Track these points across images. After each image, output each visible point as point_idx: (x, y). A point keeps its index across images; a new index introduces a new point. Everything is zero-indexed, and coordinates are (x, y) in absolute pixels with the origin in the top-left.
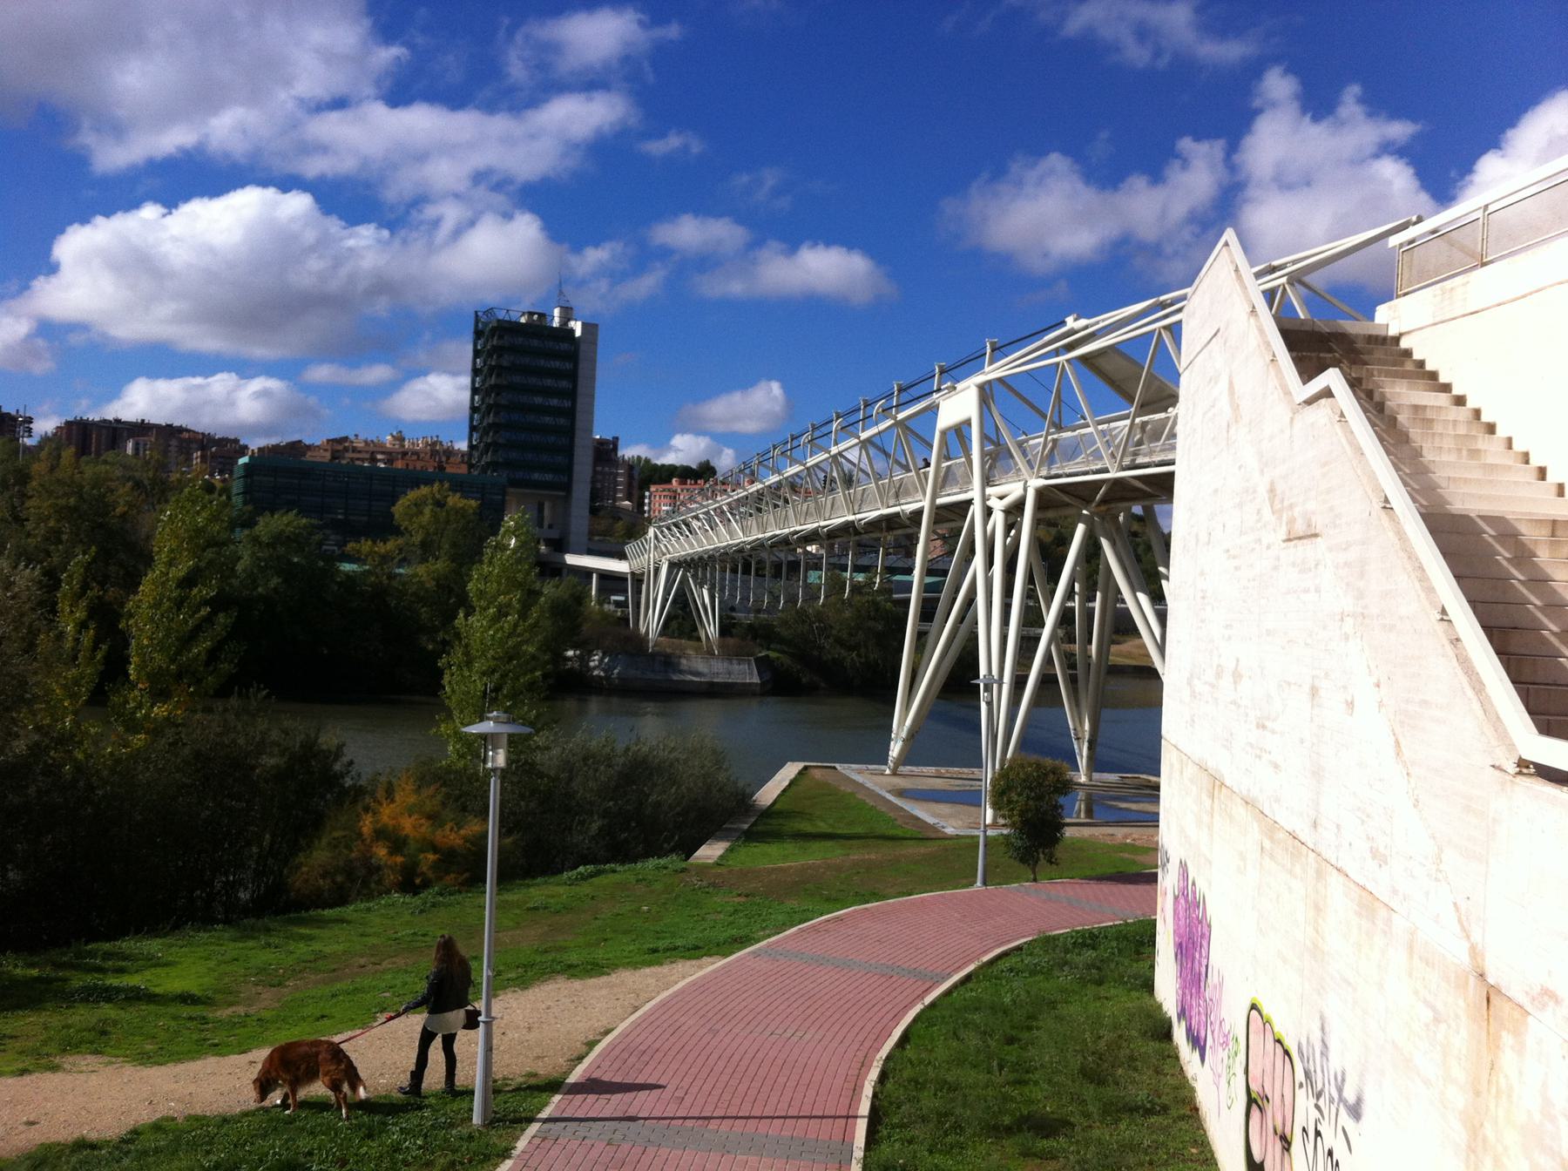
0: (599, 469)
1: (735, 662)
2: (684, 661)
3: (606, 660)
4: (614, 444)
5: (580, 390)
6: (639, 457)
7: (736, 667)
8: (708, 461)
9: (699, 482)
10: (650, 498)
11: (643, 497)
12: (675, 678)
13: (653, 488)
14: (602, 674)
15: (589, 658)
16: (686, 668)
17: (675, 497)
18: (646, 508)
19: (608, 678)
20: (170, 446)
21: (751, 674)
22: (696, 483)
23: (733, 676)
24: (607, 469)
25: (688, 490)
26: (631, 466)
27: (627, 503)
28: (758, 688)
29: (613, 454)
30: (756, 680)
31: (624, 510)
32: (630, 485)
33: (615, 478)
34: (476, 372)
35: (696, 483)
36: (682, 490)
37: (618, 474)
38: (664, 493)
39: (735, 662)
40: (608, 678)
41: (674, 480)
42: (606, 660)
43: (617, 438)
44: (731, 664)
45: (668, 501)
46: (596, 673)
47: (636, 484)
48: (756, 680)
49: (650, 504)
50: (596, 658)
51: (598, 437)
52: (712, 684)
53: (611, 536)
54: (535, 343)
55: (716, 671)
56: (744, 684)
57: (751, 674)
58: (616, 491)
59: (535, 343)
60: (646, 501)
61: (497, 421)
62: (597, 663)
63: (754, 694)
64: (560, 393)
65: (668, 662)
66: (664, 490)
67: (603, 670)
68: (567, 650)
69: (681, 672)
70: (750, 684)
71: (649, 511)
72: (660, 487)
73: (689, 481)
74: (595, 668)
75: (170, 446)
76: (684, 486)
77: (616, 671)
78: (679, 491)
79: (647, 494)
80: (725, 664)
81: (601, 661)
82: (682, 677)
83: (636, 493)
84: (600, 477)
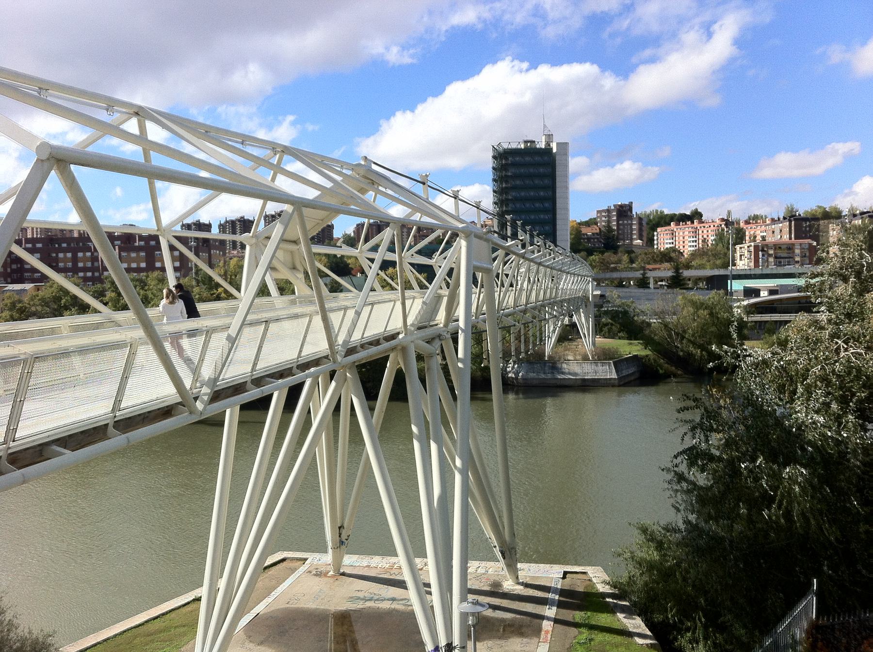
0: (620, 222)
1: (599, 364)
2: (565, 366)
3: (516, 366)
4: (630, 207)
5: (558, 184)
6: (657, 211)
7: (600, 368)
8: (697, 209)
9: (688, 223)
10: (657, 236)
11: (653, 236)
12: (559, 377)
13: (659, 230)
14: (513, 376)
15: (507, 365)
16: (567, 371)
17: (696, 232)
18: (655, 242)
19: (516, 378)
20: (403, 232)
21: (611, 372)
22: (686, 224)
23: (598, 374)
24: (625, 222)
25: (680, 229)
26: (640, 219)
27: (639, 241)
28: (616, 382)
29: (629, 213)
30: (614, 376)
31: (637, 246)
32: (640, 230)
33: (631, 227)
34: (494, 180)
35: (686, 224)
36: (677, 229)
37: (632, 224)
38: (666, 232)
39: (599, 364)
40: (516, 378)
41: (672, 223)
42: (516, 366)
43: (632, 203)
44: (597, 366)
45: (668, 236)
46: (510, 375)
47: (645, 227)
48: (614, 376)
49: (657, 239)
50: (510, 365)
51: (620, 203)
52: (584, 380)
53: (621, 264)
54: (528, 159)
55: (586, 371)
56: (606, 379)
57: (611, 372)
58: (632, 234)
59: (528, 159)
60: (655, 238)
61: (507, 209)
62: (510, 368)
63: (613, 386)
64: (544, 188)
65: (553, 365)
66: (666, 230)
67: (513, 373)
68: (461, 368)
69: (563, 373)
70: (610, 379)
71: (657, 244)
72: (663, 229)
73: (681, 223)
74: (510, 372)
75: (403, 232)
76: (678, 227)
77: (520, 374)
78: (699, 228)
79: (655, 233)
80: (593, 366)
81: (513, 368)
82: (563, 376)
83: (645, 234)
84: (621, 227)
